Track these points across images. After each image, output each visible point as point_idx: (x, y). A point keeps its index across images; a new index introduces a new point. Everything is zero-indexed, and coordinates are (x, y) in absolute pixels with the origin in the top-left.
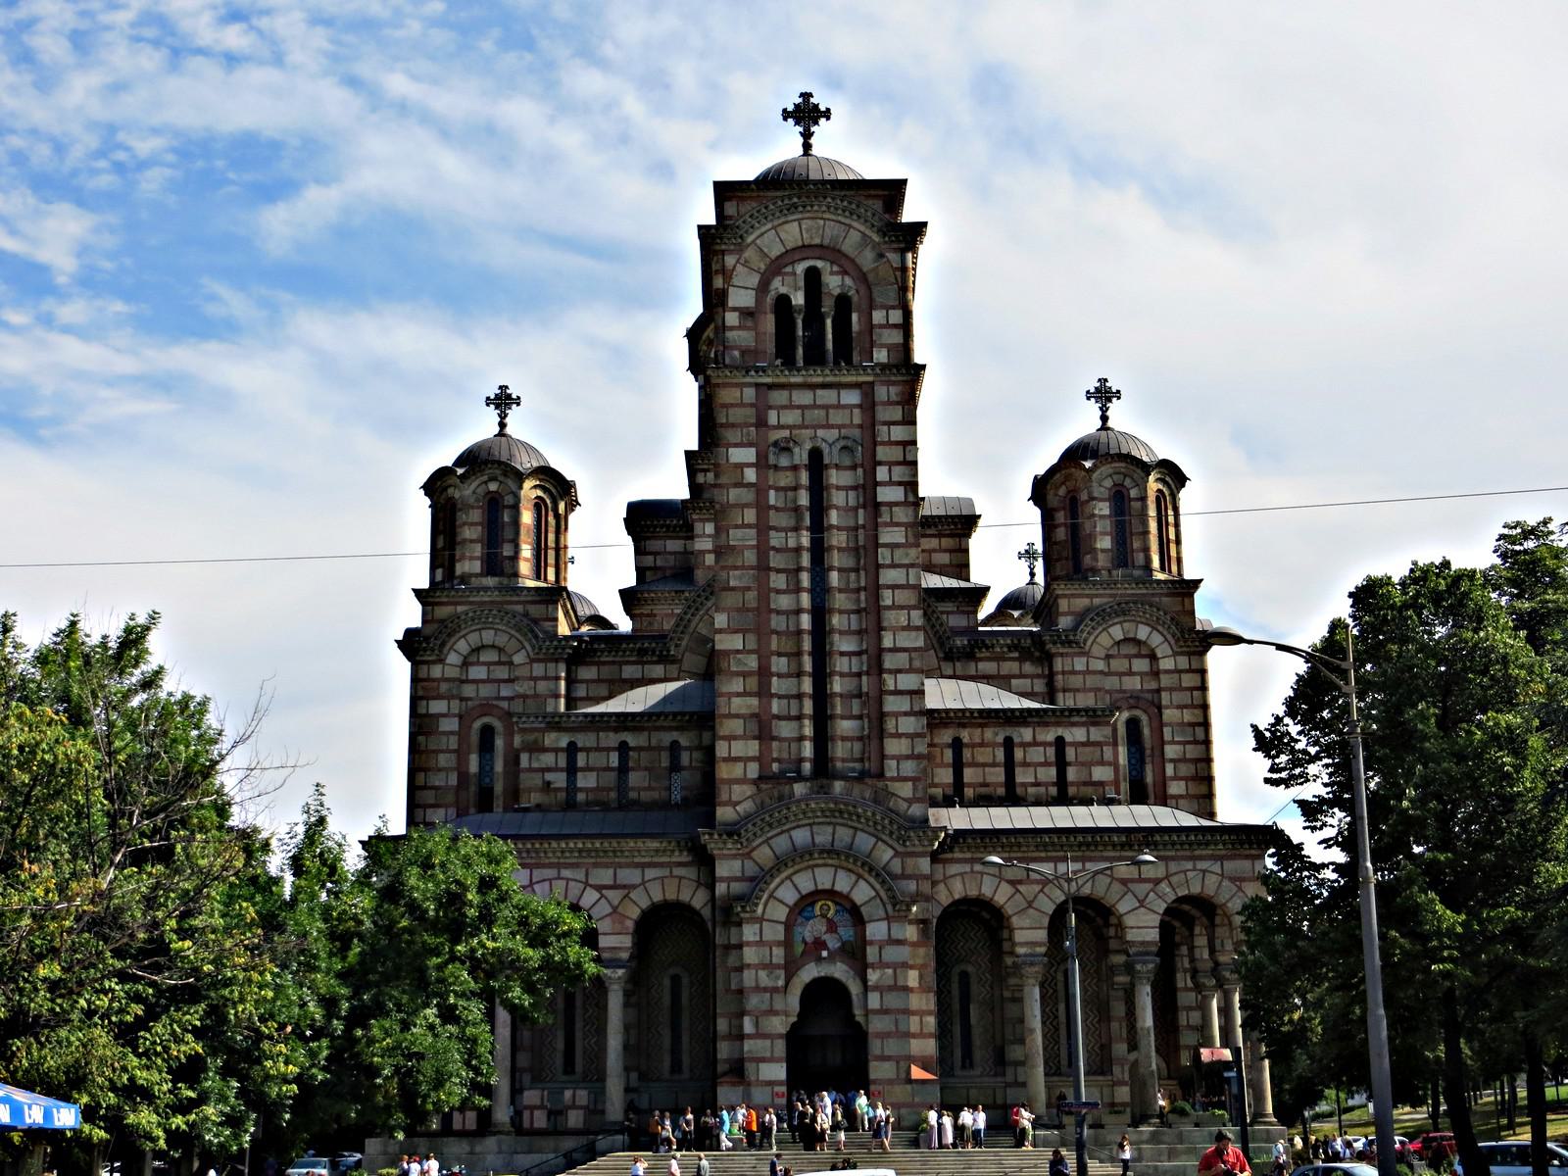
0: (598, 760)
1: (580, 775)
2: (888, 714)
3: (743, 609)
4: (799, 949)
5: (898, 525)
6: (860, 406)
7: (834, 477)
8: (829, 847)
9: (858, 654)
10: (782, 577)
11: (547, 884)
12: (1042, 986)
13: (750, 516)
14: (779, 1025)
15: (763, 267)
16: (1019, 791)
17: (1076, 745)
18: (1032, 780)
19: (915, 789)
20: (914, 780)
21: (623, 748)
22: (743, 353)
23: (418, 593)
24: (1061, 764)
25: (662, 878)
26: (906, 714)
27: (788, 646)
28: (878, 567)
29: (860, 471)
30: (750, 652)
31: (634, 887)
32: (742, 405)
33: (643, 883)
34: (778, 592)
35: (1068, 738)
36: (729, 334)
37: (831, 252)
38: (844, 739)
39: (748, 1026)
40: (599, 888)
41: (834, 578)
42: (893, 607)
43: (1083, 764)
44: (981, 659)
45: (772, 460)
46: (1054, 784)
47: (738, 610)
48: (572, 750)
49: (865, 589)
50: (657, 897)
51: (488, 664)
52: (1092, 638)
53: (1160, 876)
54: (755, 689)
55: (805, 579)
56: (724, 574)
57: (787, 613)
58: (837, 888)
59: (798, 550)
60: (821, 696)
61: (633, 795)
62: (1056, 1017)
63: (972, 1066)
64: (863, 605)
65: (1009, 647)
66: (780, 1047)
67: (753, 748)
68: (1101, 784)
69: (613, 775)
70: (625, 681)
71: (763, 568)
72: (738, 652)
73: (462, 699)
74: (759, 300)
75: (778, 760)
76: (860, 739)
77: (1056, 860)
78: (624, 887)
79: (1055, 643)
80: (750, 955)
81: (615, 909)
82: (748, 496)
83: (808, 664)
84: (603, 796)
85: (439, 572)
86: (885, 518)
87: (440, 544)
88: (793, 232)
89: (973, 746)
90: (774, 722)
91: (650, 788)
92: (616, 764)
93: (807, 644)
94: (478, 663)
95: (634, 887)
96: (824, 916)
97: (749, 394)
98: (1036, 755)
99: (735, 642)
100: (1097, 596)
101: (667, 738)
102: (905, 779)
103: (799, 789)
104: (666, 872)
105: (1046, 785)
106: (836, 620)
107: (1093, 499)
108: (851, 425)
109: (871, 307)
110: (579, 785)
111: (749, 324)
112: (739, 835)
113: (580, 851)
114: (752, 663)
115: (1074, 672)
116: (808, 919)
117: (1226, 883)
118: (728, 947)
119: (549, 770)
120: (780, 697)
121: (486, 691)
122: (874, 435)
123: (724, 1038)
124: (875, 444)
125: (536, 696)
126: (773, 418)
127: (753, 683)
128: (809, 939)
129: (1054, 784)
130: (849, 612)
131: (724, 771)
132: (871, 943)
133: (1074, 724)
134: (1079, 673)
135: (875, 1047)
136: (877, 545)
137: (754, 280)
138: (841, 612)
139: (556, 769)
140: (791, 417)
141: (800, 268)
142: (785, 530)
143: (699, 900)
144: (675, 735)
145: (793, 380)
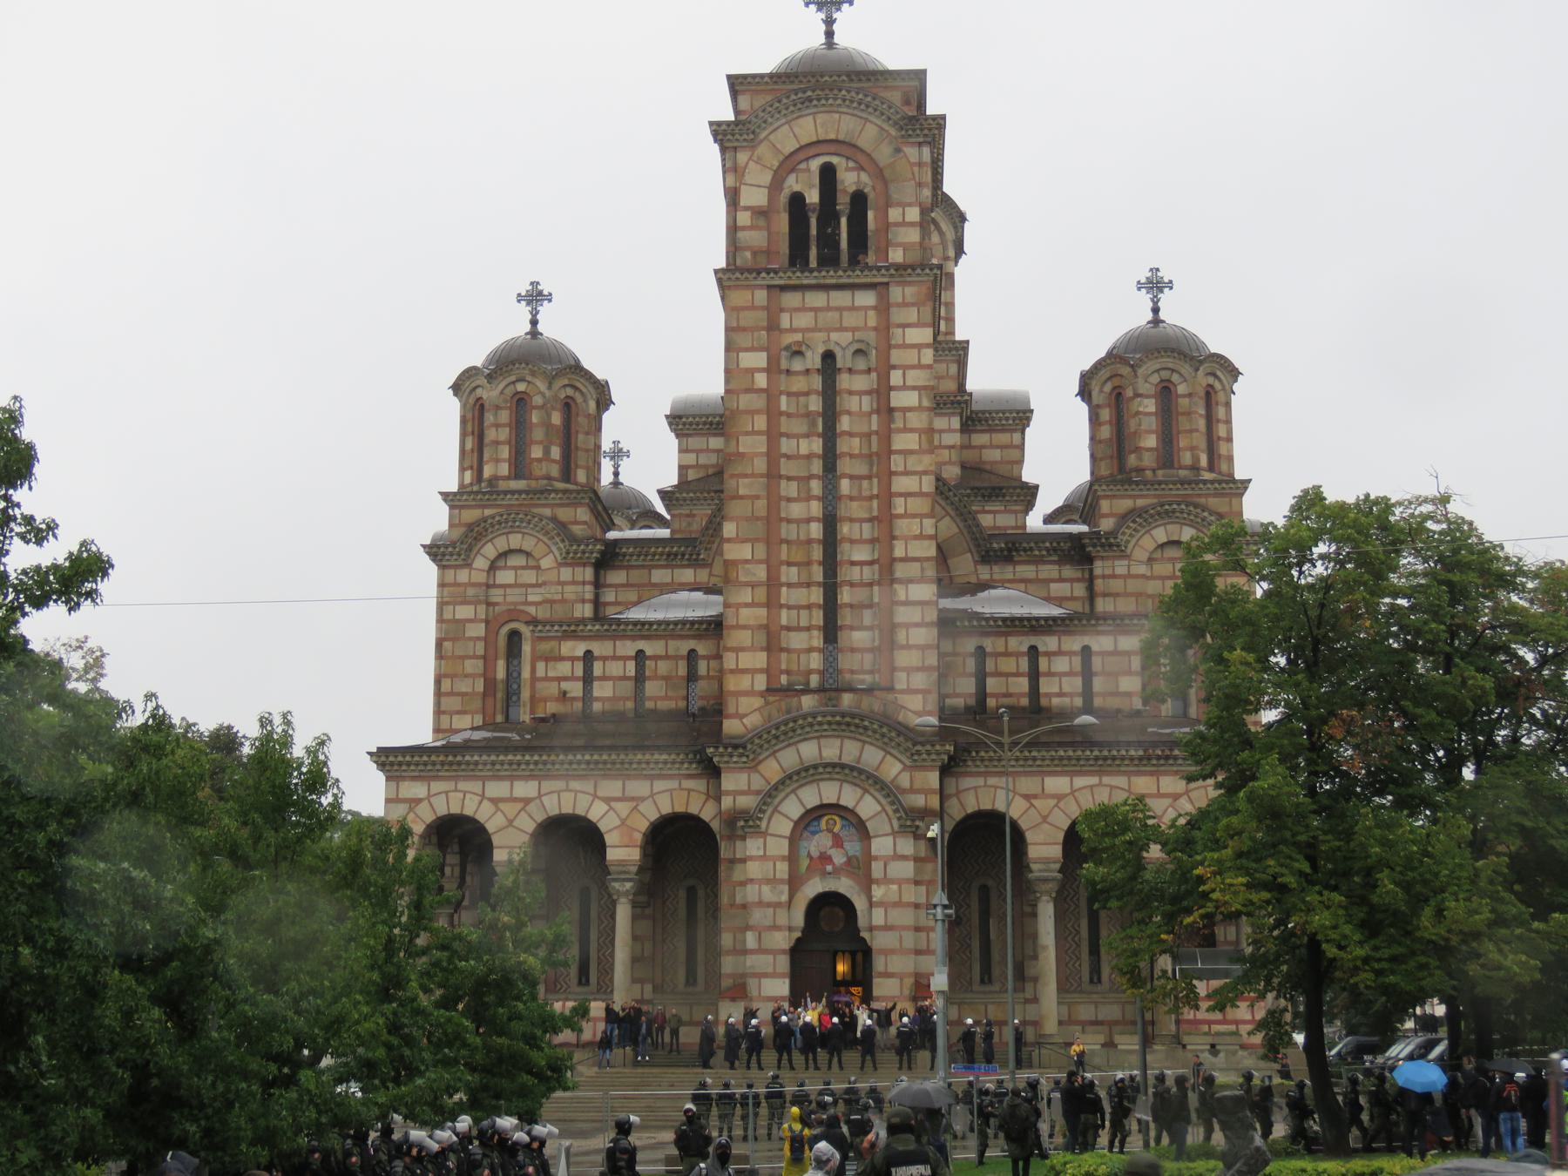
0: (615, 669)
1: (596, 684)
3: (753, 518)
4: (805, 863)
5: (912, 430)
6: (875, 308)
7: (844, 381)
8: (836, 760)
9: (871, 563)
10: (794, 484)
11: (555, 796)
12: (1056, 901)
13: (761, 422)
14: (783, 940)
15: (776, 164)
16: (1044, 702)
17: (1103, 654)
18: (1056, 690)
19: (924, 703)
20: (924, 692)
21: (640, 654)
22: (755, 254)
23: (446, 496)
24: (1087, 674)
25: (671, 791)
26: (917, 625)
27: (799, 556)
28: (892, 474)
29: (874, 375)
30: (760, 562)
31: (643, 799)
32: (753, 308)
33: (652, 795)
34: (789, 500)
35: (1095, 648)
37: (846, 146)
38: (853, 650)
39: (751, 940)
40: (607, 800)
41: (845, 486)
42: (905, 515)
44: (1020, 563)
45: (784, 364)
46: (1078, 695)
47: (747, 519)
48: (588, 657)
49: (877, 496)
50: (666, 809)
51: (515, 568)
54: (764, 599)
55: (816, 487)
56: (733, 482)
57: (798, 521)
58: (842, 803)
59: (809, 457)
60: (831, 606)
61: (649, 705)
62: (1078, 932)
63: (990, 981)
64: (875, 513)
65: (1048, 550)
66: (784, 963)
67: (761, 660)
68: (1129, 694)
69: (630, 685)
70: (655, 585)
71: (773, 475)
72: (747, 561)
73: (488, 604)
74: (771, 198)
75: (788, 672)
76: (871, 650)
77: (1072, 774)
78: (633, 799)
79: (1094, 546)
80: (754, 869)
81: (623, 822)
82: (759, 402)
83: (818, 573)
84: (620, 706)
85: (468, 474)
86: (899, 424)
87: (469, 445)
88: (807, 128)
90: (784, 633)
91: (666, 698)
92: (633, 673)
93: (817, 553)
94: (506, 567)
95: (643, 799)
96: (829, 830)
97: (761, 296)
98: (1061, 664)
99: (745, 552)
100: (1141, 496)
101: (684, 647)
102: (916, 692)
103: (808, 702)
104: (673, 784)
105: (1071, 695)
106: (845, 529)
107: (1137, 395)
108: (866, 328)
109: (888, 205)
110: (596, 694)
111: (762, 222)
112: (744, 748)
113: (588, 763)
114: (761, 573)
115: (1114, 576)
116: (814, 833)
118: (733, 861)
119: (565, 679)
120: (789, 607)
121: (514, 596)
122: (888, 339)
123: (728, 953)
124: (890, 347)
125: (563, 601)
126: (785, 321)
127: (761, 594)
128: (815, 854)
129: (1078, 695)
130: (862, 521)
131: (731, 684)
132: (876, 858)
133: (1099, 633)
134: (1120, 577)
135: (879, 964)
136: (890, 452)
137: (767, 178)
138: (852, 520)
139: (572, 678)
140: (804, 320)
141: (815, 165)
142: (797, 436)
143: (707, 813)
144: (692, 644)
145: (805, 282)
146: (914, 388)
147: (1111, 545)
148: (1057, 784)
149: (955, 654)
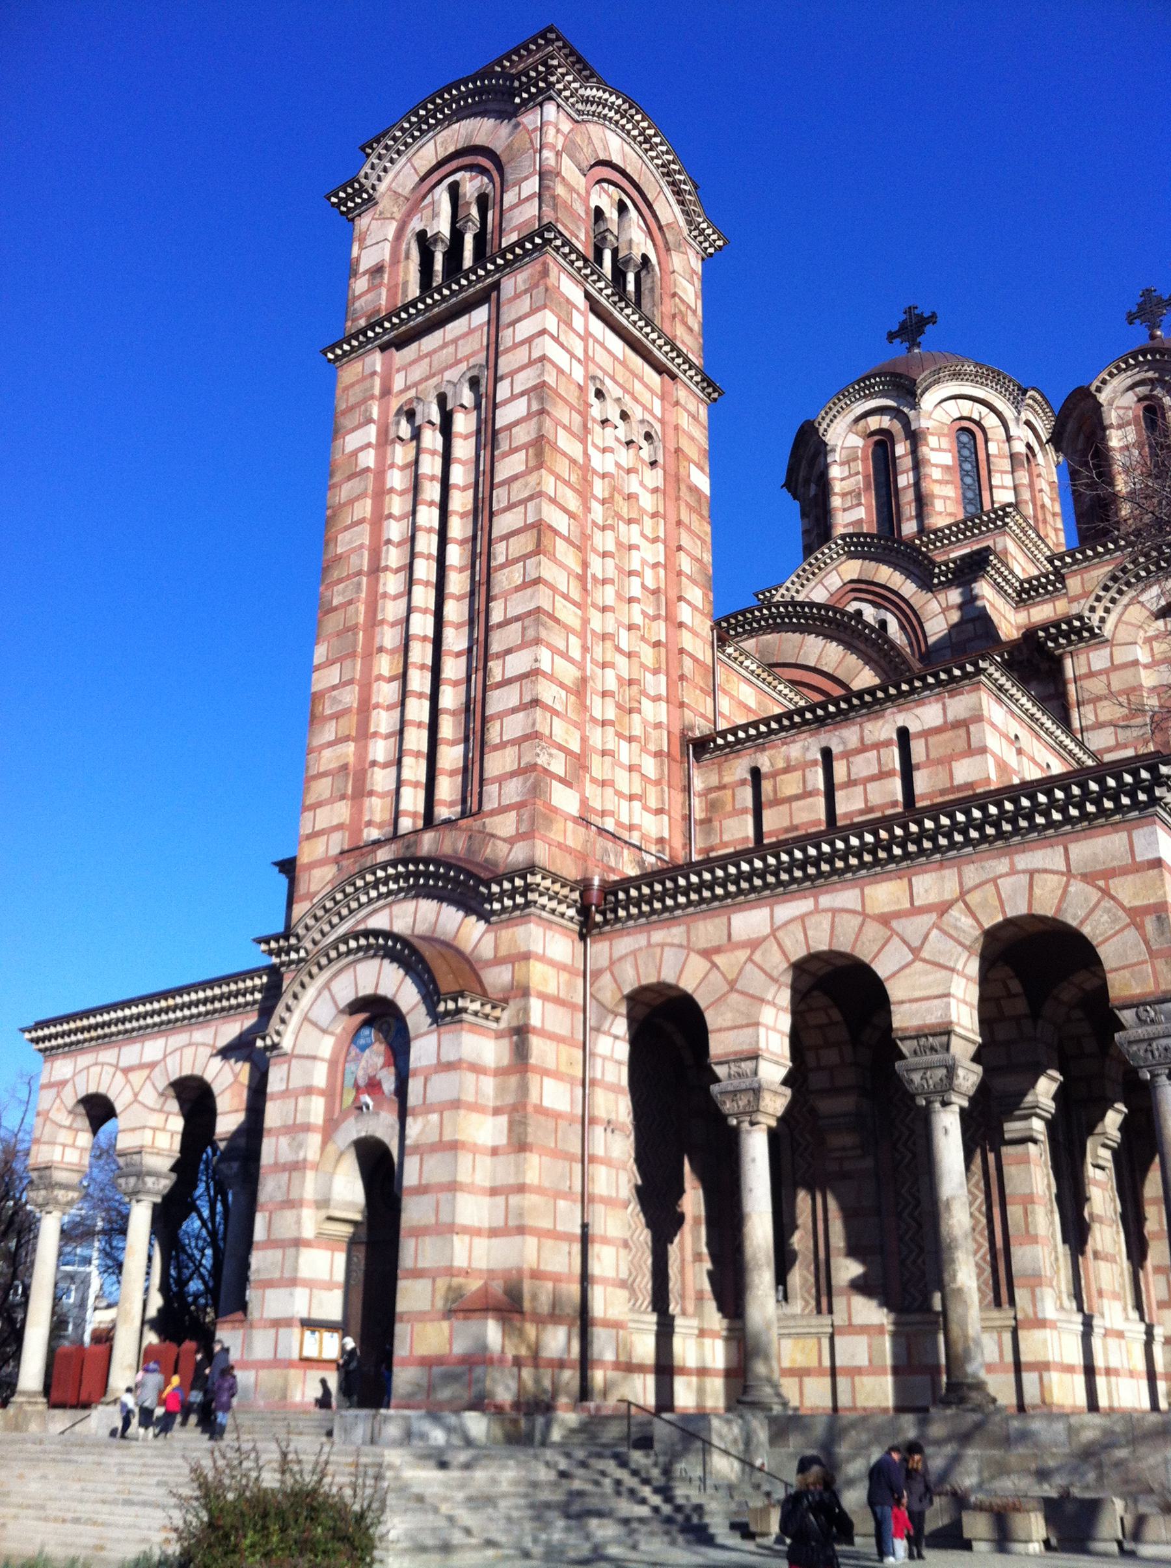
2: (493, 717)
5: (516, 450)
17: (926, 734)
20: (519, 806)
22: (369, 317)
24: (907, 771)
26: (514, 710)
36: (357, 305)
43: (939, 762)
52: (1111, 620)
53: (948, 896)
72: (334, 688)
86: (504, 446)
89: (774, 775)
98: (864, 765)
115: (1091, 674)
117: (1076, 887)
126: (398, 382)
128: (362, 1082)
133: (920, 703)
146: (522, 394)
147: (1078, 632)
148: (750, 921)
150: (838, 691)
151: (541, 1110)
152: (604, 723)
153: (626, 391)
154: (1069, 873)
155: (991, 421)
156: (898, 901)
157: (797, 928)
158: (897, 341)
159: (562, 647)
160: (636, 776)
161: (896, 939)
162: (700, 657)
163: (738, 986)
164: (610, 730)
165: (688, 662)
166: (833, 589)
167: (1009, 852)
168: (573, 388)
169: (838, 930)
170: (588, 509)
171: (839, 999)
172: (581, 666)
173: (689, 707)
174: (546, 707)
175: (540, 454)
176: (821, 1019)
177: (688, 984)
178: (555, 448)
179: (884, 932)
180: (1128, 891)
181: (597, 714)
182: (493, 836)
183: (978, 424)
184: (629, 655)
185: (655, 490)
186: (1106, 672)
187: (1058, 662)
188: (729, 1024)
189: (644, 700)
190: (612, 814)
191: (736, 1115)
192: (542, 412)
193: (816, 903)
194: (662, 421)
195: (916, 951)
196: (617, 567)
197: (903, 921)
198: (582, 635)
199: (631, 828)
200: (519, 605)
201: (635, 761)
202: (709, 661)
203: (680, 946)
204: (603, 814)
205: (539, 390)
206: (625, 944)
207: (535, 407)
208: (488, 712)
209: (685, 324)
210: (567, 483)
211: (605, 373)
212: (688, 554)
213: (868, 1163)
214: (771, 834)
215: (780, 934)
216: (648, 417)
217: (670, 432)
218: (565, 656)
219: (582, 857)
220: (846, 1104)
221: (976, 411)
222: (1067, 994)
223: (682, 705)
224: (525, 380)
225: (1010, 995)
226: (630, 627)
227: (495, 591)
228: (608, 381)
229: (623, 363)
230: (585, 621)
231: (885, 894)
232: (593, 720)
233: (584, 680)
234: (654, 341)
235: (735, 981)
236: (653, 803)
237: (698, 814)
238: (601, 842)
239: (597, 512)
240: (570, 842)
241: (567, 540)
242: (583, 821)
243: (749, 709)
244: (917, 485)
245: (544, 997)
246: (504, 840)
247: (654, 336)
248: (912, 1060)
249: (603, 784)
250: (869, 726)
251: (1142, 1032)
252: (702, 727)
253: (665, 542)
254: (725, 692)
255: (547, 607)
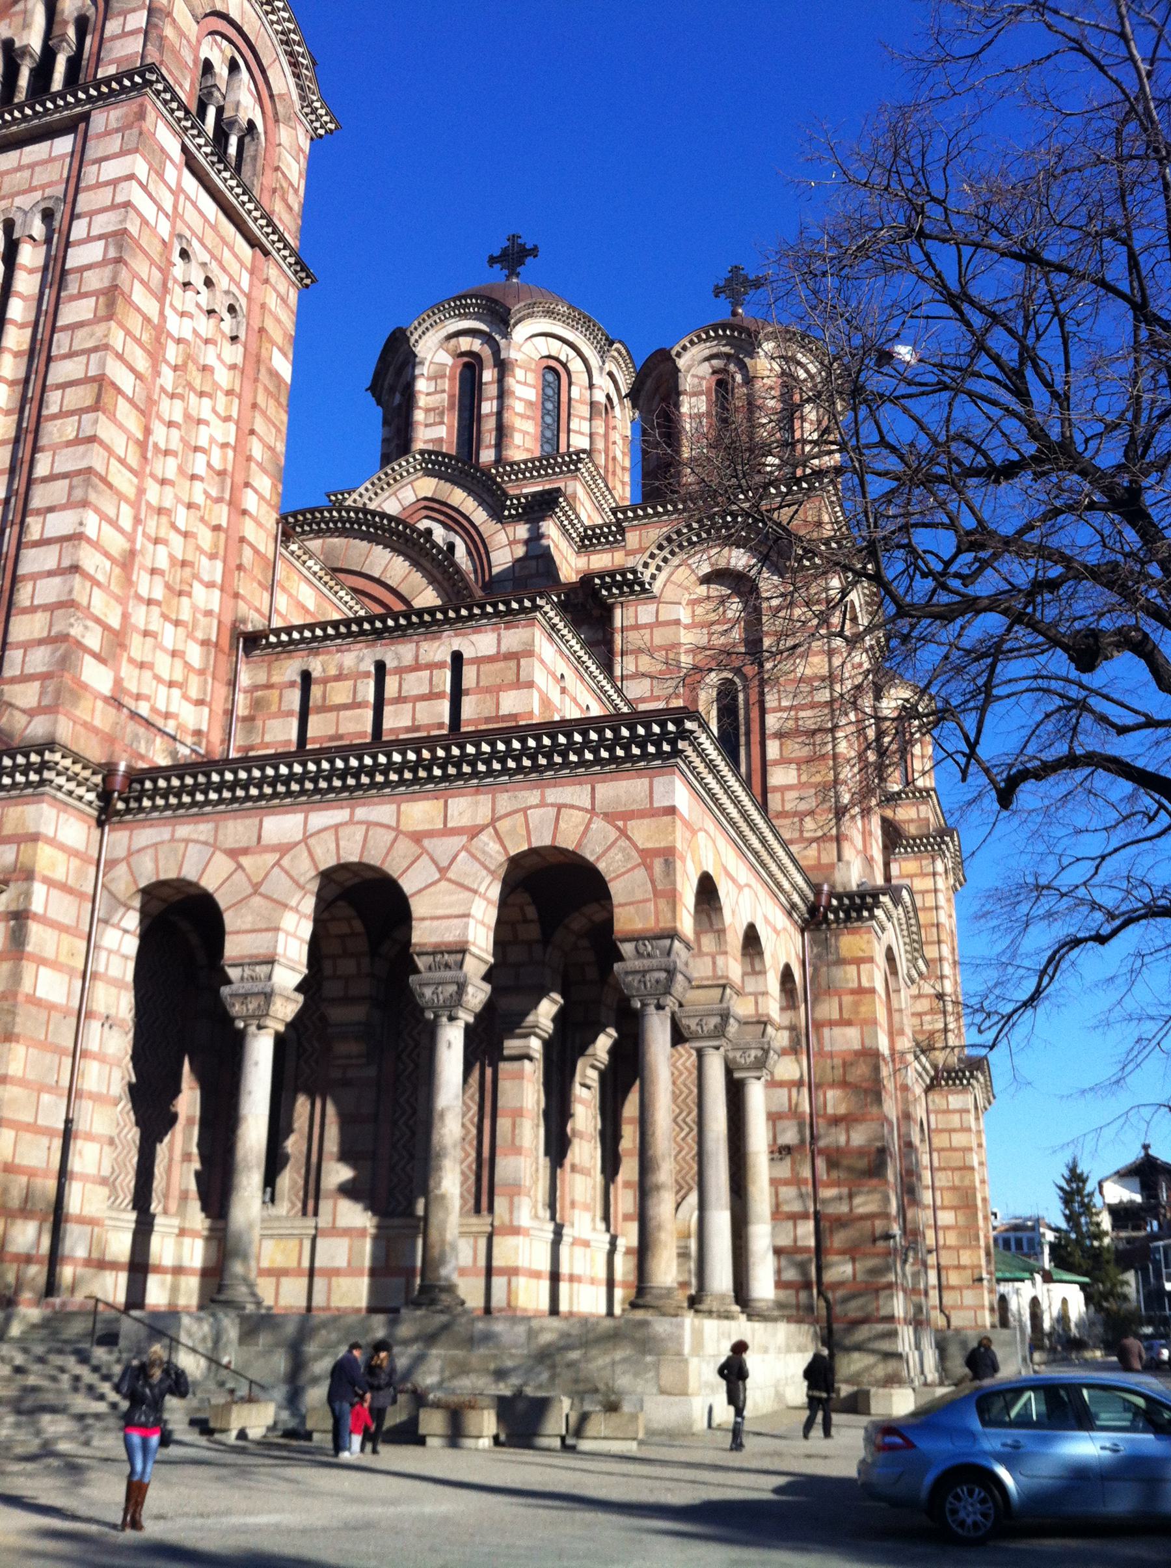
17: (479, 661)
19: (42, 694)
20: (44, 677)
26: (50, 574)
43: (487, 690)
52: (662, 577)
86: (72, 288)
89: (325, 681)
98: (416, 684)
115: (637, 627)
117: (598, 824)
133: (477, 630)
134: (645, 626)
146: (99, 237)
147: (631, 585)
148: (282, 826)
149: (269, 686)
150: (399, 607)
151: (33, 1000)
152: (150, 602)
153: (213, 256)
154: (592, 811)
155: (576, 365)
156: (432, 821)
157: (329, 836)
158: (498, 266)
159: (112, 513)
160: (178, 663)
161: (425, 858)
162: (262, 549)
163: (262, 889)
164: (155, 610)
165: (248, 553)
166: (406, 503)
167: (541, 785)
168: (157, 242)
169: (370, 843)
170: (157, 374)
171: (363, 911)
172: (131, 539)
173: (244, 599)
174: (86, 576)
175: (111, 305)
176: (344, 929)
177: (209, 883)
178: (129, 302)
179: (415, 850)
180: (643, 833)
181: (144, 591)
182: (10, 705)
183: (565, 365)
184: (186, 535)
185: (233, 367)
186: (650, 626)
187: (609, 610)
188: (248, 926)
189: (196, 584)
190: (147, 698)
191: (244, 1018)
192: (119, 260)
193: (352, 814)
194: (248, 296)
195: (443, 871)
196: (182, 439)
197: (435, 840)
198: (135, 505)
199: (167, 716)
200: (68, 461)
201: (180, 647)
202: (271, 556)
203: (206, 843)
204: (138, 697)
205: (119, 237)
206: (146, 836)
207: (112, 254)
208: (20, 572)
209: (285, 201)
210: (138, 341)
211: (194, 233)
212: (261, 439)
213: (372, 1072)
214: (315, 740)
215: (311, 841)
216: (234, 289)
217: (256, 309)
218: (114, 524)
219: (110, 739)
220: (356, 1013)
221: (565, 353)
222: (578, 922)
223: (236, 595)
224: (104, 223)
225: (526, 921)
226: (190, 506)
227: (43, 441)
228: (195, 242)
229: (214, 228)
230: (141, 491)
231: (420, 812)
232: (138, 597)
233: (132, 553)
234: (249, 212)
235: (261, 883)
236: (194, 693)
237: (241, 710)
238: (132, 727)
239: (167, 378)
240: (97, 723)
241: (131, 401)
242: (115, 701)
243: (307, 611)
244: (499, 414)
245: (50, 882)
246: (24, 711)
247: (251, 206)
248: (426, 975)
249: (142, 665)
250: (425, 645)
251: (638, 964)
252: (254, 623)
253: (237, 423)
254: (284, 589)
255: (99, 467)
